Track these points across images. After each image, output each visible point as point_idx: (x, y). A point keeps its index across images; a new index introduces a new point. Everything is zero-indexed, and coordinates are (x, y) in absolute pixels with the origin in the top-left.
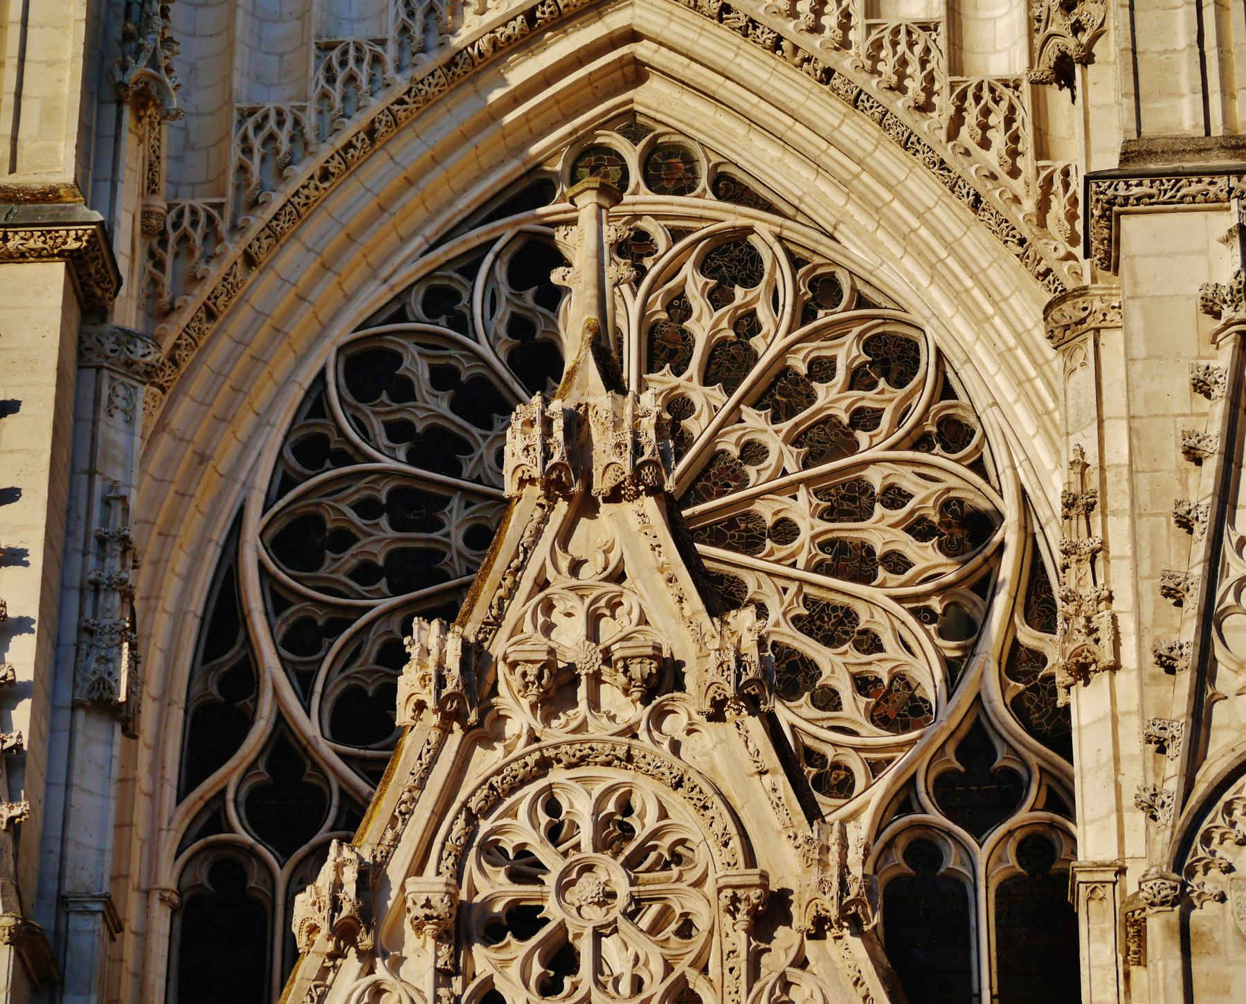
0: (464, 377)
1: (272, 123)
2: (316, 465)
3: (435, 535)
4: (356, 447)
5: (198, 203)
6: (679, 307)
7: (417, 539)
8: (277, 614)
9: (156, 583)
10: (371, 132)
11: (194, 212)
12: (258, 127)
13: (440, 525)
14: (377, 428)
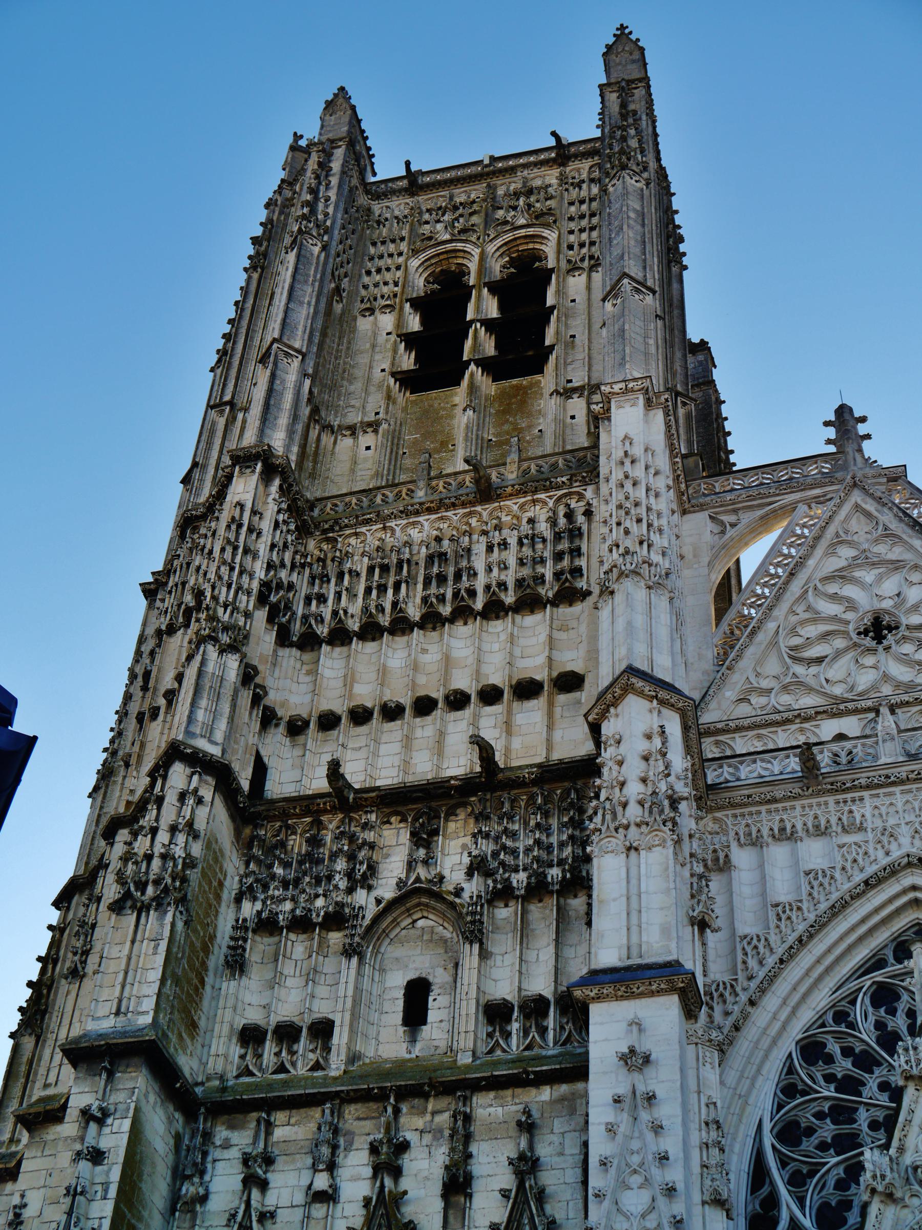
0: (857, 1050)
1: (755, 941)
2: (793, 1097)
3: (854, 1126)
4: (811, 1087)
5: (726, 980)
7: (846, 1128)
8: (783, 1168)
9: (732, 1146)
10: (800, 940)
11: (724, 983)
12: (749, 943)
13: (855, 1121)
14: (819, 1076)
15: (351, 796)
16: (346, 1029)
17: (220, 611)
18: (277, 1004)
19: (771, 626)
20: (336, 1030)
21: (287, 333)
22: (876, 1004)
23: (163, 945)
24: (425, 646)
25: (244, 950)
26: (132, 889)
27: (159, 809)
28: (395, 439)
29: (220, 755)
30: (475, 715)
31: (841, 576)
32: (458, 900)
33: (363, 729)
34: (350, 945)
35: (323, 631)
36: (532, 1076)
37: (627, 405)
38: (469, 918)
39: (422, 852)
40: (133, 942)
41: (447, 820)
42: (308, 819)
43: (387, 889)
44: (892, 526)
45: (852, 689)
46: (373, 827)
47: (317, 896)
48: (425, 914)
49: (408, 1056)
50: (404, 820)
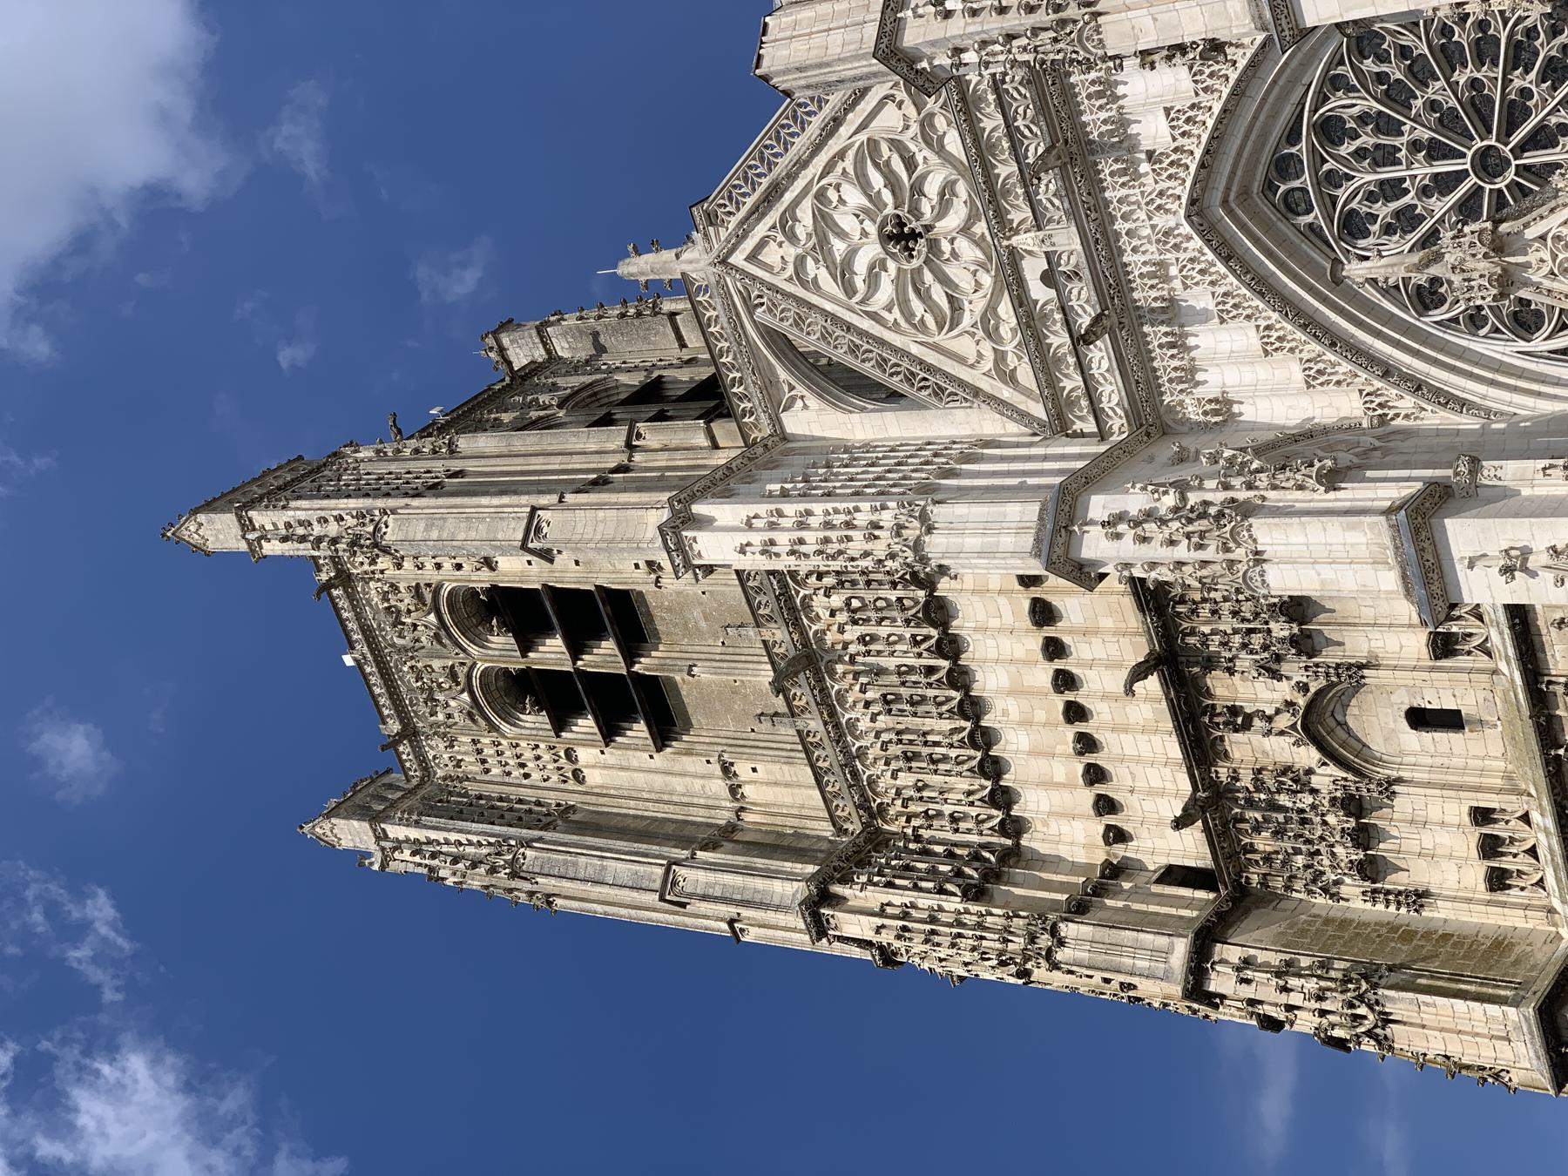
1: (1312, 373)
6: (1360, 154)
16: (1479, 795)
17: (1011, 946)
19: (915, 349)
20: (1482, 805)
21: (645, 884)
22: (1366, 234)
23: (1422, 998)
24: (999, 712)
25: (1400, 893)
26: (1363, 1029)
27: (1261, 1002)
28: (741, 745)
29: (1185, 940)
31: (843, 274)
35: (998, 815)
36: (1517, 621)
37: (696, 547)
38: (1334, 679)
39: (1257, 722)
40: (1424, 1027)
43: (1308, 756)
44: (770, 223)
45: (981, 265)
46: (1235, 771)
47: (1325, 823)
49: (1500, 728)
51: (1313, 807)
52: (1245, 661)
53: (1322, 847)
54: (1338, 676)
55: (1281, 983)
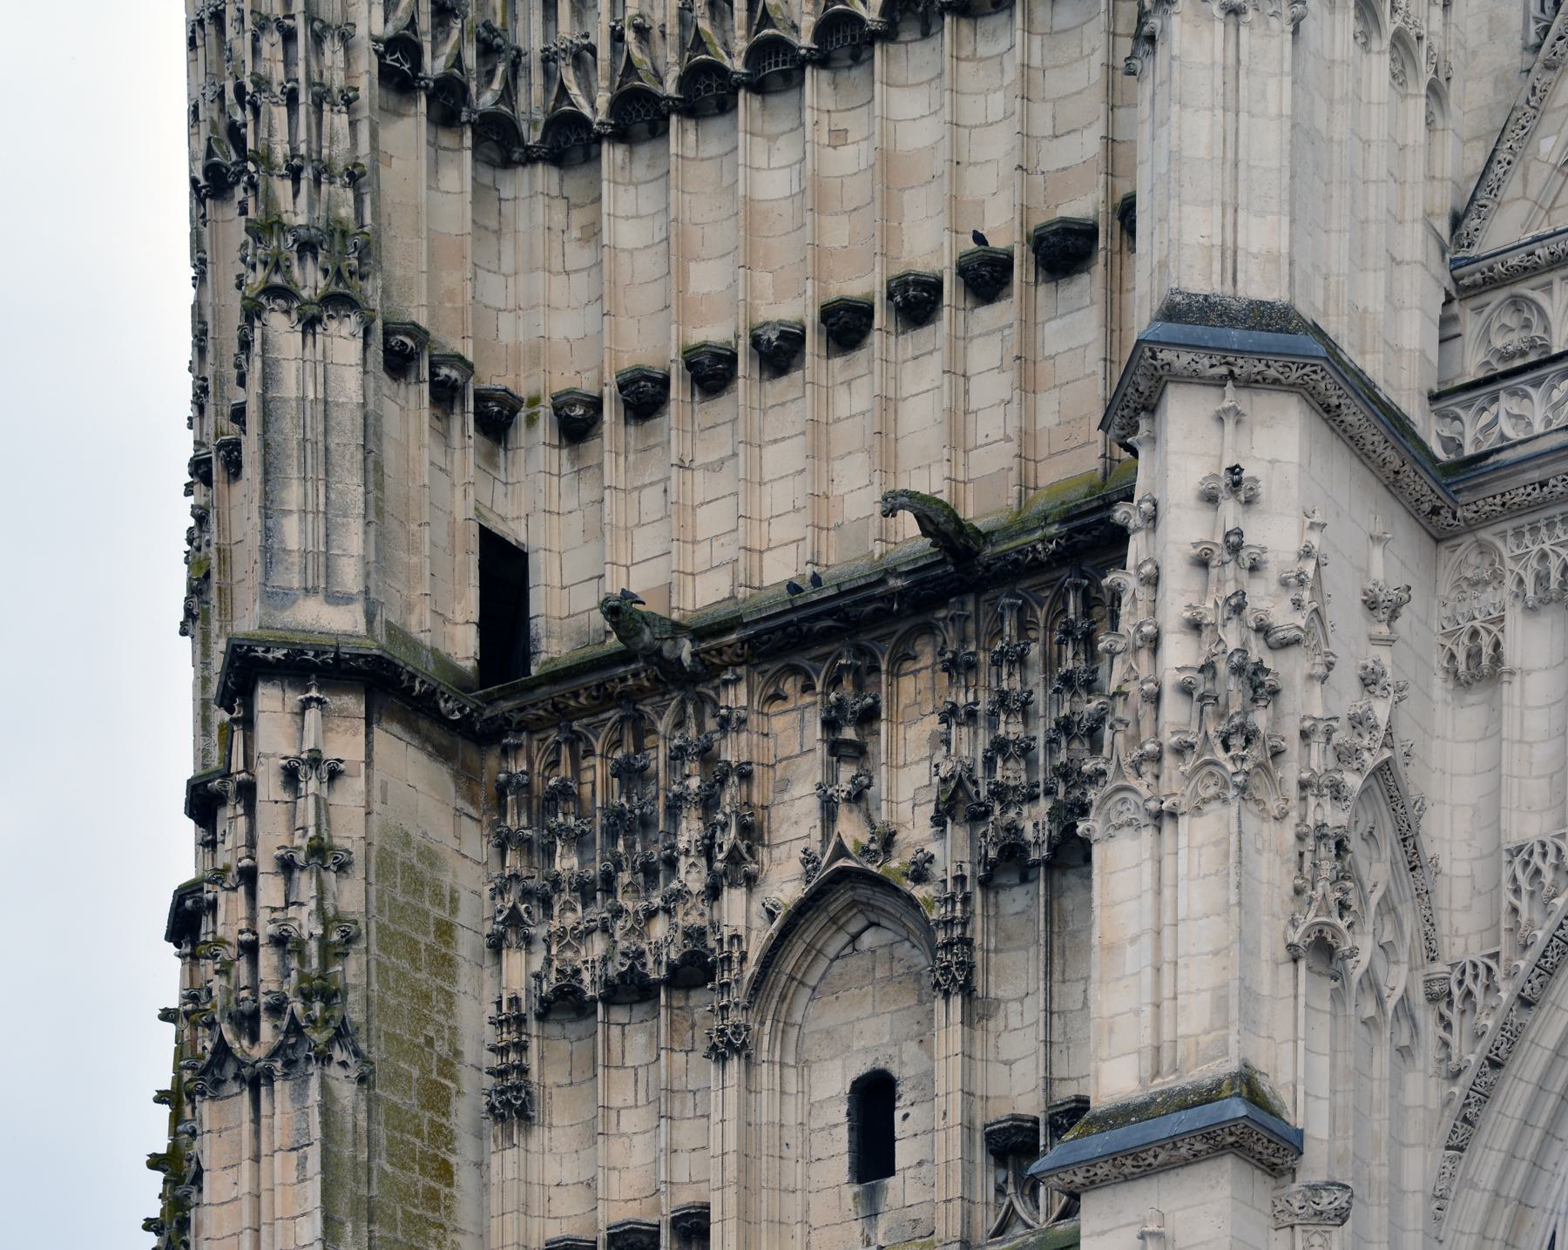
15: (686, 650)
18: (607, 1181)
23: (314, 1155)
26: (228, 1036)
30: (953, 338)
32: (919, 892)
33: (721, 406)
34: (722, 1032)
38: (941, 937)
39: (847, 772)
40: (256, 1158)
41: (895, 674)
42: (613, 715)
47: (651, 914)
48: (874, 918)
50: (808, 688)
51: (680, 895)
52: (970, 745)
53: (598, 911)
54: (948, 946)
55: (300, 858)
